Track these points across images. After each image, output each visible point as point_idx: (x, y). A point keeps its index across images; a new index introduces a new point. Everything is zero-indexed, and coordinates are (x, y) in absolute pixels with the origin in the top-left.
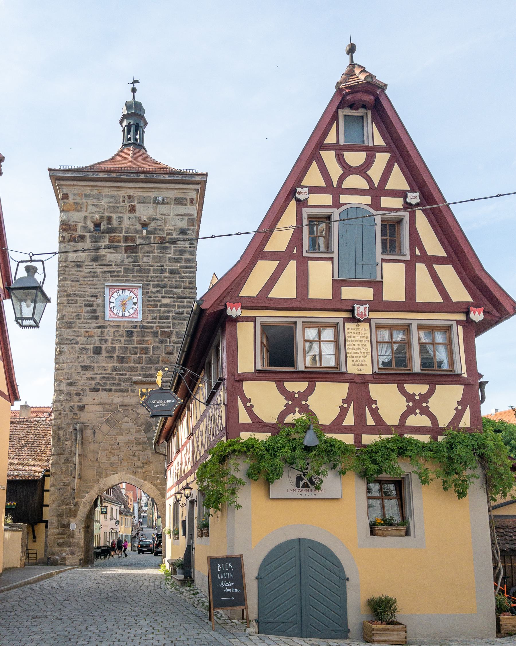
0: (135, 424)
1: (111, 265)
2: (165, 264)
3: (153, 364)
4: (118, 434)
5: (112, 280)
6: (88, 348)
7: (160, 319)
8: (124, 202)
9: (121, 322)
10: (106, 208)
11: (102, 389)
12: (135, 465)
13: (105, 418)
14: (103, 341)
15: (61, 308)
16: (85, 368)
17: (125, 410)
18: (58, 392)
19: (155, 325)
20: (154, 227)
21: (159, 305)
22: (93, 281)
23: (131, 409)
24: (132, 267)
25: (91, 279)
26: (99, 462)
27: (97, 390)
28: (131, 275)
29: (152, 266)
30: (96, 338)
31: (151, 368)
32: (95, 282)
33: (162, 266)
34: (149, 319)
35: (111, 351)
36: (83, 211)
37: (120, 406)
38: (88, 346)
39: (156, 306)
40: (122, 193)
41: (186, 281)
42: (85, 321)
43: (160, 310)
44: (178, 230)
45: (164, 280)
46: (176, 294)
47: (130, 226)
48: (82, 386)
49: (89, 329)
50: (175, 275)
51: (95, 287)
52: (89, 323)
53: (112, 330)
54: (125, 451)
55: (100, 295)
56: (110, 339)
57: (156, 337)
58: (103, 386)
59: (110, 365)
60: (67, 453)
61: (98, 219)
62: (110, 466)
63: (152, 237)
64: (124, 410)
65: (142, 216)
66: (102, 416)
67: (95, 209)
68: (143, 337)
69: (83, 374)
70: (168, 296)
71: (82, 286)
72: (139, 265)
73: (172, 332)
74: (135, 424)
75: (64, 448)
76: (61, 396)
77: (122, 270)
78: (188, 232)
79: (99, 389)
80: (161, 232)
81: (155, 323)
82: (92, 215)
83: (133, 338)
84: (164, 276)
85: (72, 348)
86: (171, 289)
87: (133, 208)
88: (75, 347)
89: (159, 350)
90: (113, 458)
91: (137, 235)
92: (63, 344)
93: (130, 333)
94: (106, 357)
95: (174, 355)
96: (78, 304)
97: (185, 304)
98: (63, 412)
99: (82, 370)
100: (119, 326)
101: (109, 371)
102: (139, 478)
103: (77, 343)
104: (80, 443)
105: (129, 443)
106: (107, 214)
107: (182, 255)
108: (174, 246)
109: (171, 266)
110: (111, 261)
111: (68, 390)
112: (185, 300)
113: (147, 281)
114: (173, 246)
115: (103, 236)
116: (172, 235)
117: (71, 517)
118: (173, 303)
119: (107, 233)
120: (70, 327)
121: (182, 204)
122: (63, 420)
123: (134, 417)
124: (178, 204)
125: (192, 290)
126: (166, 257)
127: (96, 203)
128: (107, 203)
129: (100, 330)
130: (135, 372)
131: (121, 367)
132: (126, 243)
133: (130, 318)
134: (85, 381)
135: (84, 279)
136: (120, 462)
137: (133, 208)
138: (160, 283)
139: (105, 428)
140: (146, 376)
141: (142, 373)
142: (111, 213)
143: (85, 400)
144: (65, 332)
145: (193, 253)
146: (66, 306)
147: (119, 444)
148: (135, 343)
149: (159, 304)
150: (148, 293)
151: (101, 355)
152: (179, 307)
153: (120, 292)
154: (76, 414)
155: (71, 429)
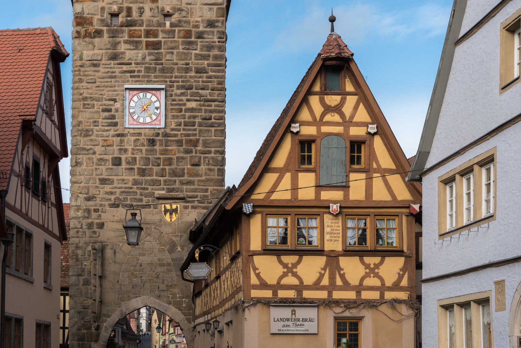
2: (190, 62)
3: (177, 177)
4: (140, 254)
5: (132, 81)
6: (106, 158)
7: (185, 126)
11: (123, 204)
12: (159, 288)
14: (123, 151)
15: (77, 113)
16: (104, 181)
17: (147, 228)
18: (76, 208)
19: (179, 133)
21: (183, 110)
22: (111, 82)
23: (153, 227)
25: (109, 80)
26: (121, 285)
27: (117, 206)
28: (153, 75)
30: (115, 147)
31: (175, 181)
32: (113, 83)
34: (173, 126)
35: (131, 163)
38: (106, 157)
39: (181, 110)
41: (214, 81)
42: (103, 128)
43: (185, 115)
45: (189, 81)
46: (203, 97)
49: (107, 137)
50: (202, 75)
51: (113, 89)
52: (107, 131)
53: (133, 138)
54: (148, 273)
55: (119, 99)
56: (130, 148)
57: (181, 146)
58: (124, 202)
59: (131, 178)
60: (86, 274)
62: (133, 288)
68: (166, 146)
70: (194, 99)
71: (98, 88)
73: (198, 141)
74: (158, 244)
75: (83, 268)
76: (78, 212)
77: (143, 69)
81: (180, 131)
83: (156, 147)
85: (89, 159)
86: (197, 91)
88: (93, 158)
89: (184, 161)
92: (79, 154)
93: (152, 142)
94: (126, 169)
95: (200, 167)
96: (95, 109)
97: (213, 108)
98: (80, 230)
99: (101, 184)
100: (140, 134)
101: (130, 185)
103: (94, 153)
104: (100, 263)
105: (152, 264)
109: (198, 64)
111: (86, 206)
112: (213, 103)
113: (171, 82)
117: (92, 342)
118: (199, 107)
120: (86, 136)
122: (81, 239)
125: (221, 92)
129: (119, 138)
130: (157, 186)
133: (152, 125)
135: (100, 80)
136: (142, 285)
138: (185, 84)
140: (170, 190)
141: (165, 187)
143: (105, 217)
144: (82, 141)
146: (82, 111)
147: (141, 266)
148: (158, 153)
149: (184, 108)
150: (171, 95)
151: (120, 167)
152: (206, 111)
153: (141, 95)
154: (94, 232)
155: (90, 248)
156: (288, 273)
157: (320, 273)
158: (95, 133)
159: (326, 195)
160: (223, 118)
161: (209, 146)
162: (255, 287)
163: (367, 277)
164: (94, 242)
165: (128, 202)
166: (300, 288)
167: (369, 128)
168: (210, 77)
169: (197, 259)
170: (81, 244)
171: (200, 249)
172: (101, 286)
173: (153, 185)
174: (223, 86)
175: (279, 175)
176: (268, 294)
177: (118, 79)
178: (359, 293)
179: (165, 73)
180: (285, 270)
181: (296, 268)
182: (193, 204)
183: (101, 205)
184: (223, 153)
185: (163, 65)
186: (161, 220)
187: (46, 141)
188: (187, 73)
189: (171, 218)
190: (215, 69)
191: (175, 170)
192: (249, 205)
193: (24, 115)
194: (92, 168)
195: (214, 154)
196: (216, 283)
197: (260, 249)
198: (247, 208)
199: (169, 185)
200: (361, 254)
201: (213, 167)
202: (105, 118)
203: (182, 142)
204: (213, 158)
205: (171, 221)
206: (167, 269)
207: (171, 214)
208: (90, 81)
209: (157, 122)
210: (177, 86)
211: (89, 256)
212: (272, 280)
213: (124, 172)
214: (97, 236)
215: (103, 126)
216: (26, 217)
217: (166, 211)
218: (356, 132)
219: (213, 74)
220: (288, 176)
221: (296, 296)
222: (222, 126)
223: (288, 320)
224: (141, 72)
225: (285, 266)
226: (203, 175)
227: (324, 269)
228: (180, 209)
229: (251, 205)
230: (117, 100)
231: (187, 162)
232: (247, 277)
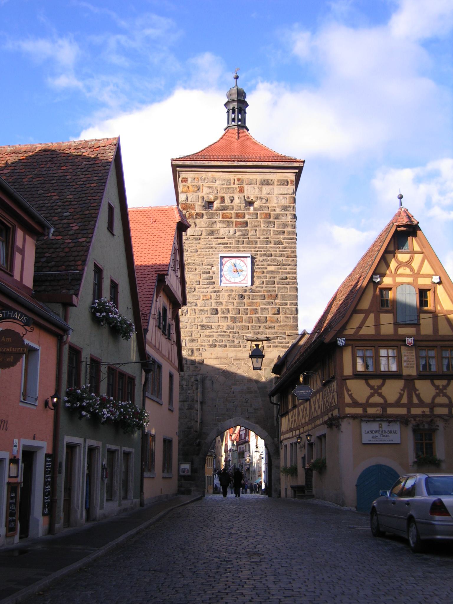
1: (224, 238)
2: (269, 236)
5: (225, 250)
6: (205, 309)
7: (266, 284)
11: (219, 345)
12: (248, 411)
14: (219, 303)
19: (262, 289)
20: (260, 205)
23: (243, 362)
24: (241, 239)
25: (207, 250)
27: (215, 346)
28: (241, 246)
29: (259, 238)
30: (212, 301)
31: (260, 327)
38: (206, 308)
40: (231, 176)
41: (288, 251)
43: (266, 276)
44: (280, 207)
49: (206, 293)
51: (210, 257)
53: (227, 294)
59: (225, 324)
61: (212, 198)
62: (227, 411)
63: (258, 214)
64: (237, 364)
68: (252, 300)
70: (273, 264)
71: (200, 256)
77: (233, 242)
83: (244, 301)
84: (269, 246)
86: (275, 258)
89: (266, 311)
93: (242, 296)
94: (221, 317)
96: (197, 272)
97: (288, 270)
100: (232, 291)
101: (224, 329)
106: (219, 195)
107: (284, 228)
108: (277, 220)
112: (288, 267)
113: (255, 251)
114: (276, 220)
115: (217, 213)
116: (276, 211)
119: (220, 210)
124: (280, 185)
128: (219, 185)
129: (215, 294)
132: (237, 219)
134: (203, 338)
137: (241, 189)
138: (266, 253)
141: (252, 331)
145: (295, 227)
147: (233, 393)
148: (246, 305)
149: (265, 270)
151: (217, 316)
152: (282, 273)
155: (193, 379)
156: (375, 393)
157: (400, 393)
158: (197, 290)
159: (402, 331)
160: (295, 278)
161: (285, 299)
162: (349, 405)
163: (438, 396)
164: (196, 374)
165: (223, 343)
166: (385, 406)
167: (433, 279)
169: (302, 382)
170: (185, 377)
171: (304, 374)
172: (202, 409)
173: (242, 330)
174: (295, 254)
175: (365, 315)
176: (359, 411)
178: (432, 410)
180: (372, 391)
181: (381, 389)
183: (202, 346)
185: (249, 238)
187: (173, 292)
188: (267, 244)
190: (289, 242)
191: (259, 317)
192: (342, 339)
194: (194, 317)
195: (290, 305)
196: (305, 404)
197: (351, 374)
198: (341, 342)
199: (255, 330)
200: (432, 377)
208: (193, 251)
209: (244, 282)
210: (260, 254)
211: (192, 386)
212: (362, 400)
213: (220, 319)
214: (198, 370)
215: (203, 285)
216: (158, 350)
218: (423, 282)
219: (287, 245)
220: (372, 316)
221: (381, 412)
222: (295, 284)
223: (376, 432)
224: (232, 244)
225: (372, 387)
227: (403, 390)
229: (343, 339)
232: (340, 396)
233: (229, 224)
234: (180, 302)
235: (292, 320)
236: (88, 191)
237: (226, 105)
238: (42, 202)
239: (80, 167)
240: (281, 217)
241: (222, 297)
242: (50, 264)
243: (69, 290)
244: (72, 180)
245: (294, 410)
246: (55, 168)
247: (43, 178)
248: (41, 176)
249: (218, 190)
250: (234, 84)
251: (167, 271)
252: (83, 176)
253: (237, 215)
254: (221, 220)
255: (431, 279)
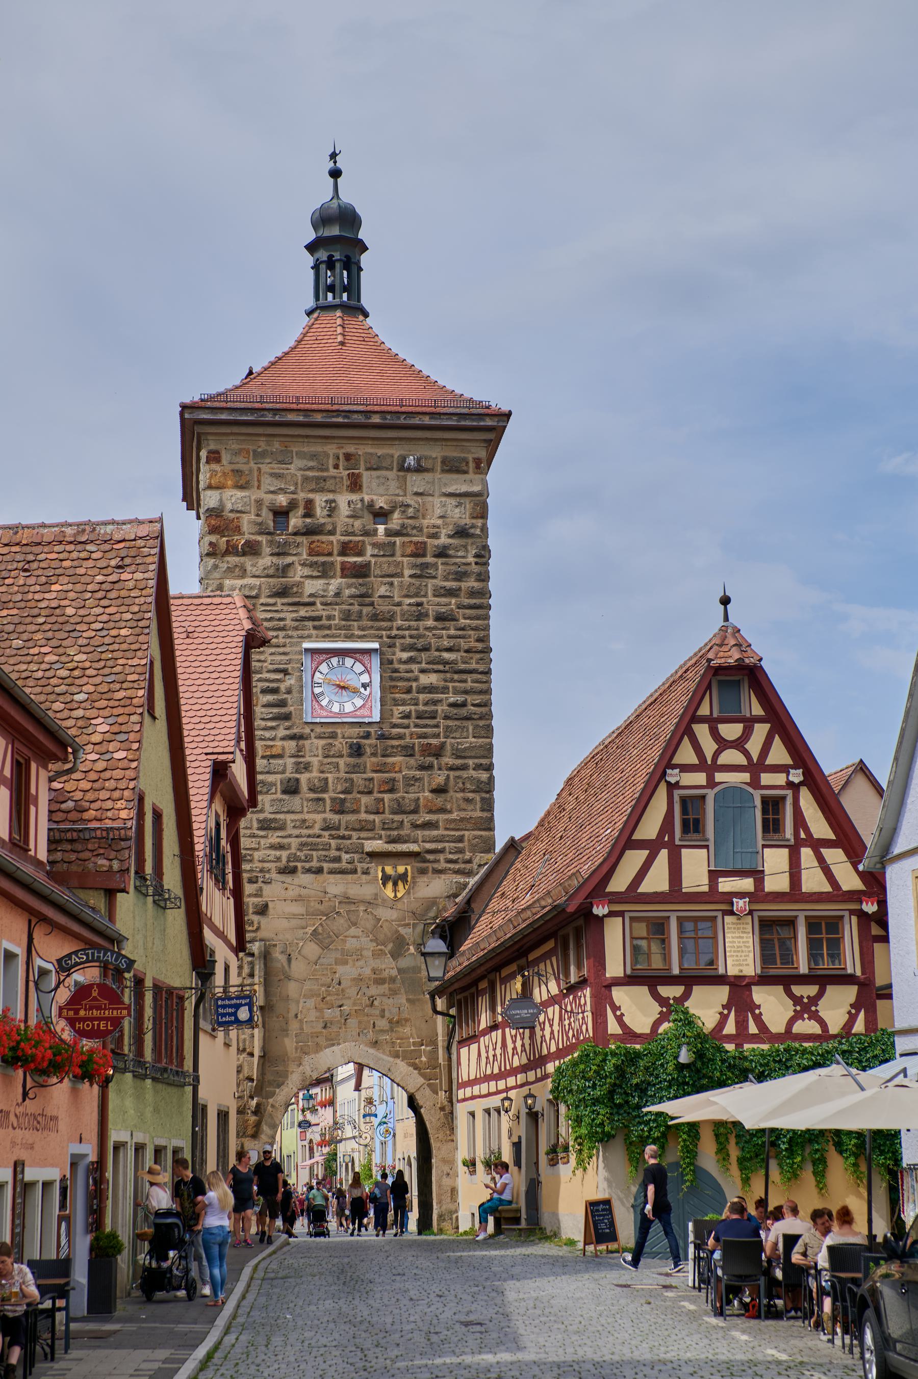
0: (371, 941)
1: (313, 604)
7: (418, 718)
8: (336, 467)
9: (337, 726)
10: (299, 482)
11: (303, 868)
12: (374, 1027)
13: (310, 929)
14: (302, 766)
23: (362, 908)
26: (301, 1021)
27: (293, 871)
28: (355, 623)
29: (399, 604)
31: (402, 821)
33: (419, 604)
36: (252, 487)
37: (340, 903)
39: (409, 691)
40: (331, 449)
41: (470, 636)
44: (451, 527)
45: (425, 635)
47: (352, 520)
48: (260, 861)
50: (447, 624)
51: (281, 650)
52: (272, 728)
57: (411, 755)
61: (284, 504)
62: (325, 1027)
63: (398, 543)
64: (348, 912)
65: (375, 498)
66: (303, 923)
67: (278, 484)
68: (383, 756)
69: (262, 837)
72: (372, 604)
73: (442, 746)
77: (336, 614)
78: (472, 531)
79: (296, 867)
80: (415, 532)
81: (408, 727)
82: (271, 496)
87: (355, 480)
89: (417, 784)
90: (328, 1013)
91: (366, 539)
93: (357, 751)
97: (469, 685)
99: (260, 829)
101: (316, 830)
102: (384, 1053)
106: (302, 496)
107: (459, 580)
108: (444, 560)
109: (438, 604)
110: (311, 595)
112: (469, 677)
113: (389, 637)
114: (440, 561)
118: (442, 683)
121: (459, 471)
123: (369, 926)
124: (450, 471)
126: (426, 586)
127: (277, 471)
128: (301, 469)
129: (293, 743)
131: (340, 821)
139: (312, 950)
141: (383, 833)
142: (312, 491)
145: (484, 577)
147: (340, 984)
149: (414, 685)
153: (335, 660)
157: (721, 1013)
159: (726, 885)
160: (487, 704)
161: (463, 754)
165: (315, 864)
168: (463, 629)
171: (523, 976)
173: (360, 830)
177: (290, 633)
179: (377, 620)
182: (436, 866)
184: (489, 768)
186: (376, 894)
188: (420, 620)
189: (395, 891)
193: (213, 753)
195: (474, 769)
200: (787, 981)
201: (471, 795)
202: (268, 705)
203: (413, 748)
204: (470, 778)
205: (396, 896)
206: (390, 989)
207: (395, 884)
209: (365, 712)
214: (255, 928)
217: (386, 878)
219: (468, 621)
220: (664, 853)
224: (334, 620)
226: (454, 810)
228: (412, 873)
230: (290, 671)
231: (424, 785)
233: (325, 572)
234: (246, 804)
235: (478, 806)
236: (116, 647)
237: (311, 248)
238: (24, 667)
239: (90, 588)
240: (451, 552)
241: (311, 751)
242: (63, 806)
243: (111, 860)
244: (79, 620)
245: (494, 1034)
246: (38, 588)
247: (15, 612)
248: (11, 605)
249: (296, 484)
250: (330, 194)
251: (232, 753)
252: (100, 610)
253: (345, 550)
254: (307, 560)
255: (784, 775)
